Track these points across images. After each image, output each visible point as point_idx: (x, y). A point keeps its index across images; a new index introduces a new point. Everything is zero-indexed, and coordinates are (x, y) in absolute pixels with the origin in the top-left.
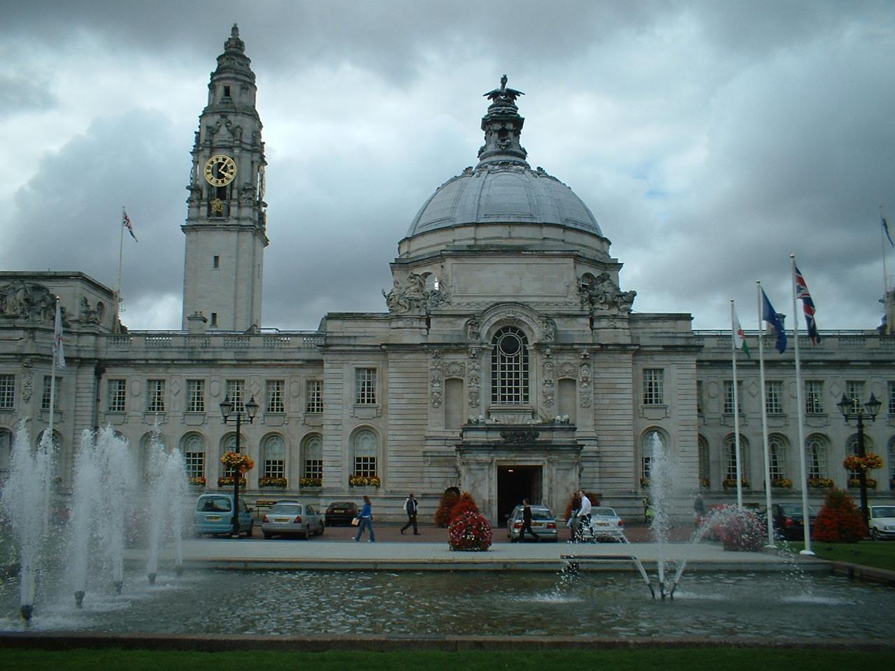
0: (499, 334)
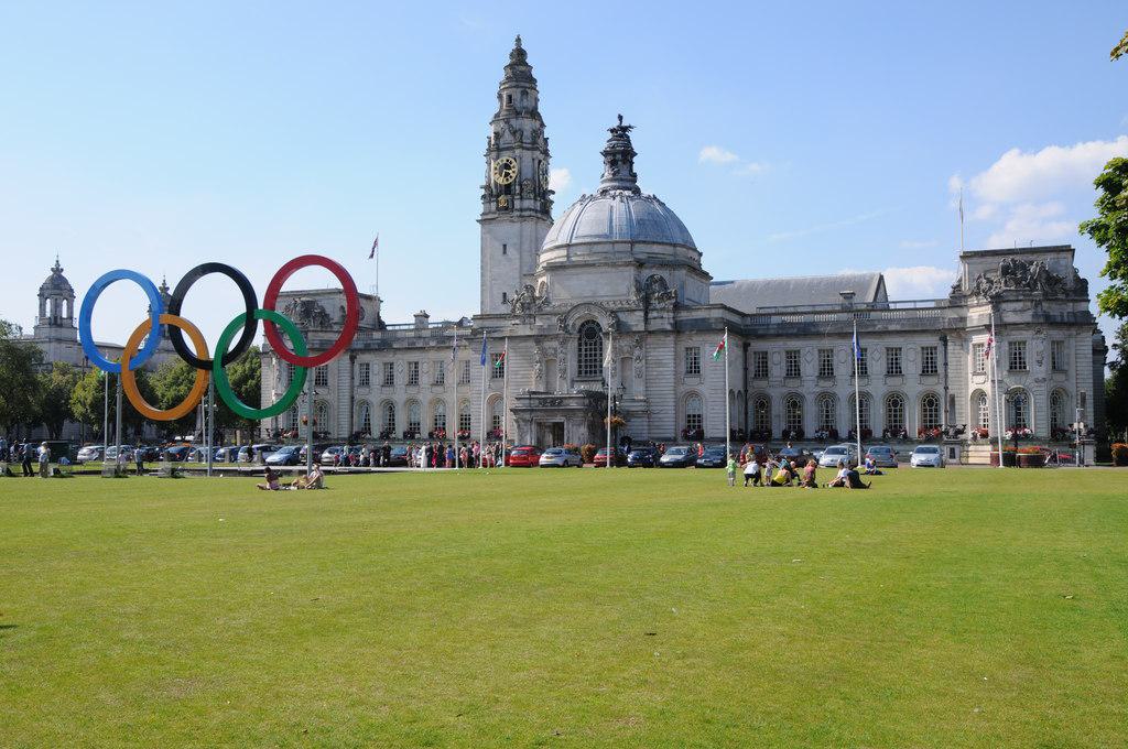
0: (583, 325)
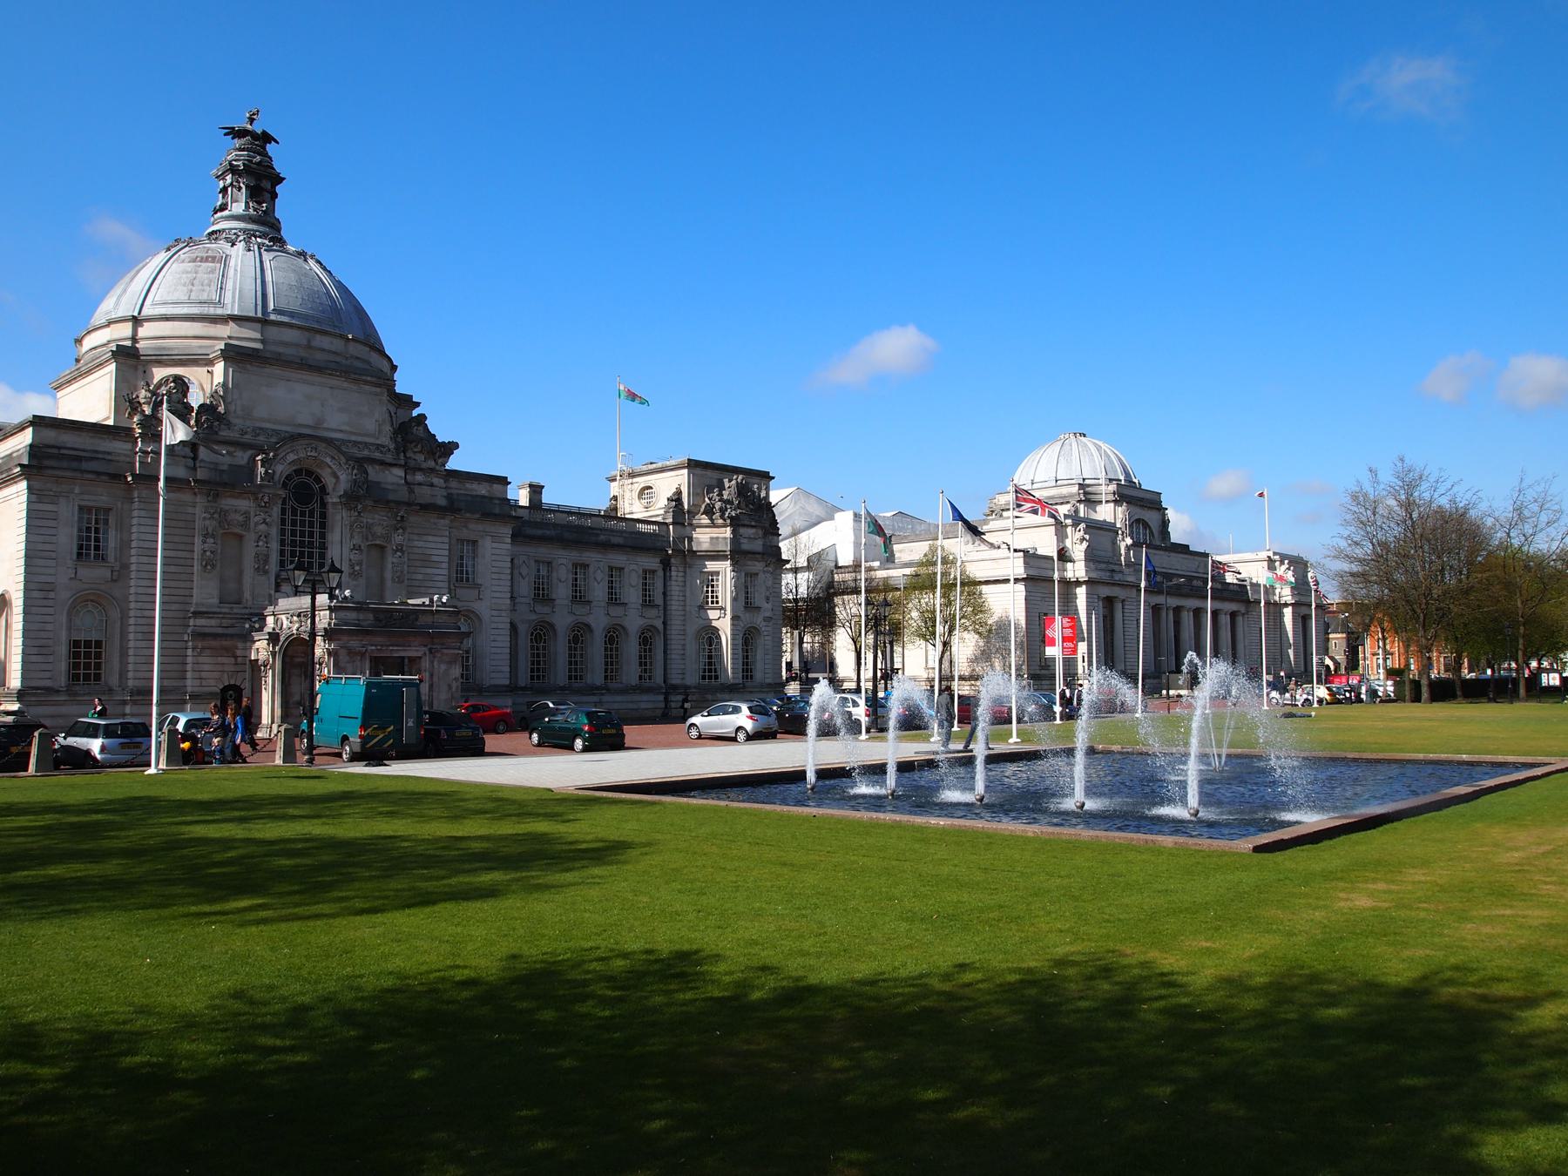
0: (288, 477)
